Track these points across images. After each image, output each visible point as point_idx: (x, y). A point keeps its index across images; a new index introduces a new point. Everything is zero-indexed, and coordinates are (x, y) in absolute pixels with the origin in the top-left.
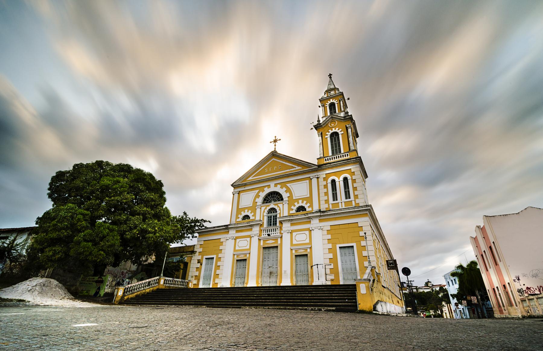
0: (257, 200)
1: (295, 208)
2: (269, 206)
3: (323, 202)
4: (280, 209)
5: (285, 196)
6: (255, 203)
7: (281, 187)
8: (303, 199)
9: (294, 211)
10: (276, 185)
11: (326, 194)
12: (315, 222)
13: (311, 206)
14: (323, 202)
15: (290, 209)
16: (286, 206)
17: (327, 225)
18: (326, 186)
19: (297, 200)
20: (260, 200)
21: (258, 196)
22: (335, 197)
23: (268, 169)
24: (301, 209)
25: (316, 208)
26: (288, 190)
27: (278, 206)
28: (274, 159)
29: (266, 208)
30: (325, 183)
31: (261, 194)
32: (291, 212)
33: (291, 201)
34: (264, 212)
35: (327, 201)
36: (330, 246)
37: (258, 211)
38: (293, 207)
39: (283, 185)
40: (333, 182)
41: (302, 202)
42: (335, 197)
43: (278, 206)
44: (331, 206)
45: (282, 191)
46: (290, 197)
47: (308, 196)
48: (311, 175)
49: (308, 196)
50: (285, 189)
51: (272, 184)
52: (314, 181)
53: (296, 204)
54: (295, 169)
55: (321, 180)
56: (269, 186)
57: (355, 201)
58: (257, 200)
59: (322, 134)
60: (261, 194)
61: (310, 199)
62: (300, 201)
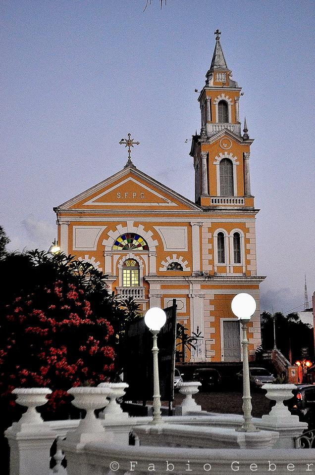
0: (105, 242)
1: (167, 264)
2: (126, 255)
3: (206, 262)
4: (144, 263)
5: (153, 244)
6: (100, 246)
7: (146, 230)
8: (179, 254)
9: (165, 269)
10: (136, 225)
11: (211, 252)
12: (196, 288)
13: (190, 264)
14: (206, 262)
15: (159, 265)
16: (153, 260)
17: (211, 293)
18: (211, 241)
19: (170, 254)
20: (109, 244)
21: (105, 236)
22: (222, 259)
23: (123, 195)
24: (176, 266)
25: (196, 268)
26: (156, 236)
27: (141, 258)
28: (130, 178)
29: (121, 258)
30: (209, 235)
31: (110, 233)
32: (161, 269)
33: (161, 254)
34: (118, 263)
35: (211, 262)
36: (213, 319)
37: (108, 259)
38: (163, 263)
39: (148, 227)
40: (221, 235)
41: (178, 258)
42: (222, 259)
43: (141, 258)
44: (216, 268)
45: (148, 236)
46: (160, 247)
47: (186, 250)
48: (193, 221)
49: (186, 250)
50: (150, 233)
51: (130, 222)
52: (196, 230)
53: (168, 258)
54: (167, 204)
55: (205, 230)
56: (125, 224)
57: (246, 267)
58: (105, 242)
59: (208, 155)
60: (110, 233)
61: (188, 256)
62: (175, 256)
